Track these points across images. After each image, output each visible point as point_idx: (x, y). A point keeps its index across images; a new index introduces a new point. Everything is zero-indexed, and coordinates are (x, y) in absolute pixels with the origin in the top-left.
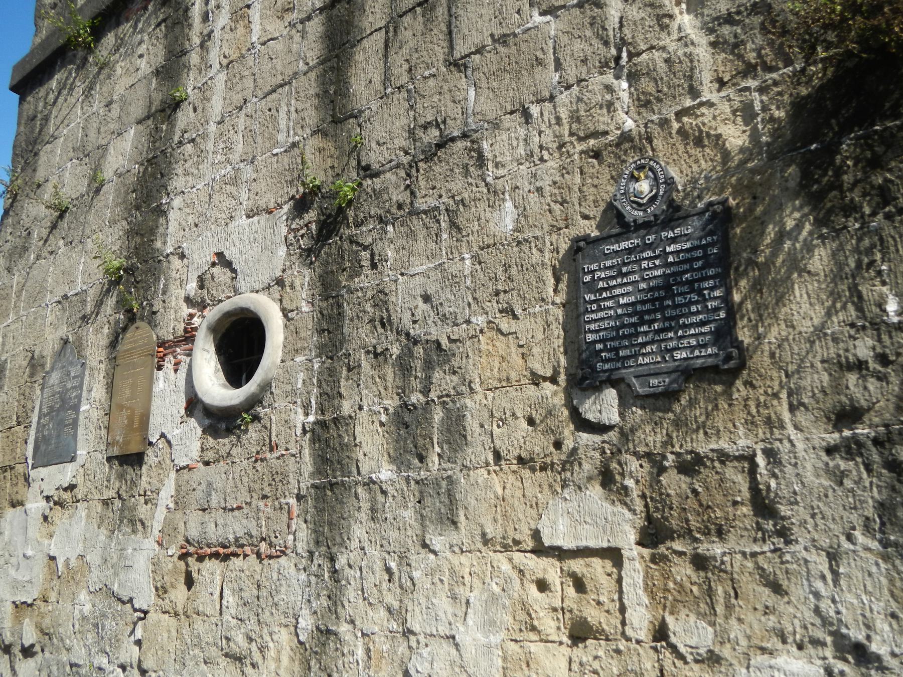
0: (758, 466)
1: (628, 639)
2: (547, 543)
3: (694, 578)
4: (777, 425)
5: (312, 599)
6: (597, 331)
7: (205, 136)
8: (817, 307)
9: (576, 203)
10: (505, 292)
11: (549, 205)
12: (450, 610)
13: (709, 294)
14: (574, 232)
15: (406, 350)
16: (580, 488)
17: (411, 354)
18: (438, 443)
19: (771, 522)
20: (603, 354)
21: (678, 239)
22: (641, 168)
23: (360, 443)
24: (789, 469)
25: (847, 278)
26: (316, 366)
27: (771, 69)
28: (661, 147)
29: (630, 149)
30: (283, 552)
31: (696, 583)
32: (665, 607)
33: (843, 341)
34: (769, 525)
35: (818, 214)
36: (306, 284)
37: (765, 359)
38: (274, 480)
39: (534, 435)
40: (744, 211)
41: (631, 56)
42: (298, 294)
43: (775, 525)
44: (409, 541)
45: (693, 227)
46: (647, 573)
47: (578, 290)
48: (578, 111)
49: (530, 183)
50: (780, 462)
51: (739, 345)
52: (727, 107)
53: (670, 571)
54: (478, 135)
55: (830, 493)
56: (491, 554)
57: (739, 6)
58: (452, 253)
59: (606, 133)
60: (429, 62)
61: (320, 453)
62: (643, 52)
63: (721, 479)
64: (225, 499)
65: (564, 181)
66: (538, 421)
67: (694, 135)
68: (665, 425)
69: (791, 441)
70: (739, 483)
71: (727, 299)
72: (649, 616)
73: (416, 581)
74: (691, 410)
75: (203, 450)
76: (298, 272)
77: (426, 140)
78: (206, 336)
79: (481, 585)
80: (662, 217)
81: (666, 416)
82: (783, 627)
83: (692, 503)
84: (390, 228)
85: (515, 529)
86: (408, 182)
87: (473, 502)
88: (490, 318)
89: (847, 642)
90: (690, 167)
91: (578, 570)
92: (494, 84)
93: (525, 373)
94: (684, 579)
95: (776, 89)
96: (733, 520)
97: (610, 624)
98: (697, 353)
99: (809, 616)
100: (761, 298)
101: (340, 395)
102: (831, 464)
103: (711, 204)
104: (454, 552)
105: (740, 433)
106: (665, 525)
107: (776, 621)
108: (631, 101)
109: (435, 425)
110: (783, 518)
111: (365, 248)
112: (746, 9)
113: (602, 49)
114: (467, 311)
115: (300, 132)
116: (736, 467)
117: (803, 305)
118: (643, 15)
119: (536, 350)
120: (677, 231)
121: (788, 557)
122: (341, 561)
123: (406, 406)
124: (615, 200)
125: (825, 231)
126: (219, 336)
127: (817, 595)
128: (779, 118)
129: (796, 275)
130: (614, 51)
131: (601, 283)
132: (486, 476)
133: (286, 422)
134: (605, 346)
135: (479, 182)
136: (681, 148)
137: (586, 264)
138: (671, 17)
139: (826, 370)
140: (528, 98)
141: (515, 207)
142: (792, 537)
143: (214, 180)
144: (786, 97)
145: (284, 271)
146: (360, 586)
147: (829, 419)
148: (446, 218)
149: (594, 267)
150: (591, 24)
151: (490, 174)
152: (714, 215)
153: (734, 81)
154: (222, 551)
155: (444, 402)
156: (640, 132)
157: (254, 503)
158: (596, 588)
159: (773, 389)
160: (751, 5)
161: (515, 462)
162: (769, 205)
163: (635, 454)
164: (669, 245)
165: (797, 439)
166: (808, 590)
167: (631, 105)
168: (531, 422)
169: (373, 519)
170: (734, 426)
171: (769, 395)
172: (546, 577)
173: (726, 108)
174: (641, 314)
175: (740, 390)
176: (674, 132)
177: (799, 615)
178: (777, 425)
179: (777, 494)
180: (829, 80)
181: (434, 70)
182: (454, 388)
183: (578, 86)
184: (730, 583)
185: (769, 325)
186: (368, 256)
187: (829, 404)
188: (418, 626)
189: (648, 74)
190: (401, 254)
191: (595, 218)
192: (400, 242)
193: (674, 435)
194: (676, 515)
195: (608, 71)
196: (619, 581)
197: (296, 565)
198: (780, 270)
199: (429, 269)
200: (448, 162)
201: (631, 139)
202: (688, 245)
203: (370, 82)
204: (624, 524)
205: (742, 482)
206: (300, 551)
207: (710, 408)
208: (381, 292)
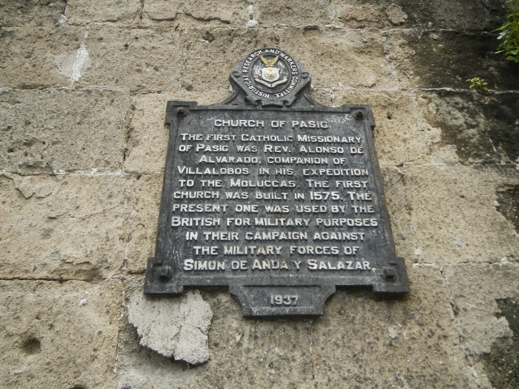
98: (340, 265)
131: (204, 156)
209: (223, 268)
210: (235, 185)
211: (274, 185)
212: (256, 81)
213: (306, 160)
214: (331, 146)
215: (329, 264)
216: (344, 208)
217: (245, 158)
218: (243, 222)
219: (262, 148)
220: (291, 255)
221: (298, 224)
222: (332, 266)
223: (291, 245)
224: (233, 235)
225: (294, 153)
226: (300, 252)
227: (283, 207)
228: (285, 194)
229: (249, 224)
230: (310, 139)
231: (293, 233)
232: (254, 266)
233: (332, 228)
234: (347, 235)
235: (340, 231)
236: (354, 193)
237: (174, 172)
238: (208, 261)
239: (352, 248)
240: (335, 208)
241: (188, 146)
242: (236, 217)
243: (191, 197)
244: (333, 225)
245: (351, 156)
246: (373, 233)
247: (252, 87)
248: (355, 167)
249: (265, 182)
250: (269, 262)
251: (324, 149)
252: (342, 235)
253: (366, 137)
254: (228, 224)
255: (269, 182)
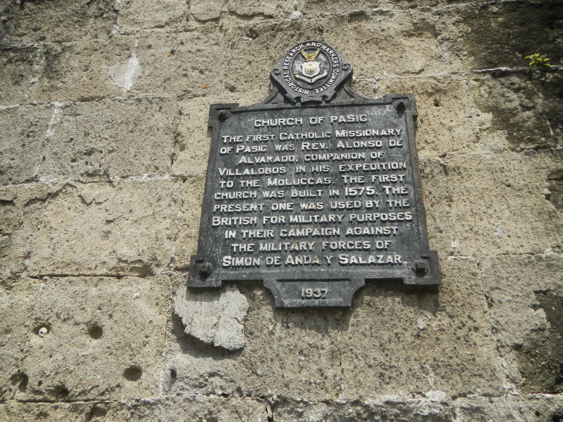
6: (230, 214)
98: (371, 259)
131: (243, 157)
209: (258, 264)
210: (272, 184)
211: (309, 183)
212: (296, 78)
213: (342, 155)
214: (369, 140)
215: (360, 259)
216: (378, 202)
217: (283, 157)
218: (278, 220)
219: (300, 146)
220: (323, 250)
221: (332, 220)
222: (363, 260)
223: (323, 240)
224: (268, 233)
225: (332, 149)
226: (332, 247)
227: (318, 204)
228: (320, 191)
229: (284, 221)
230: (348, 134)
231: (326, 230)
232: (287, 262)
233: (365, 223)
234: (380, 230)
235: (373, 226)
236: (390, 187)
237: (215, 173)
238: (245, 257)
239: (384, 242)
240: (369, 203)
241: (228, 148)
242: (272, 215)
243: (230, 197)
244: (366, 220)
245: (389, 150)
246: (407, 227)
247: (292, 84)
248: (393, 161)
249: (301, 180)
250: (301, 257)
251: (362, 143)
252: (375, 230)
253: (407, 129)
254: (264, 223)
255: (305, 179)
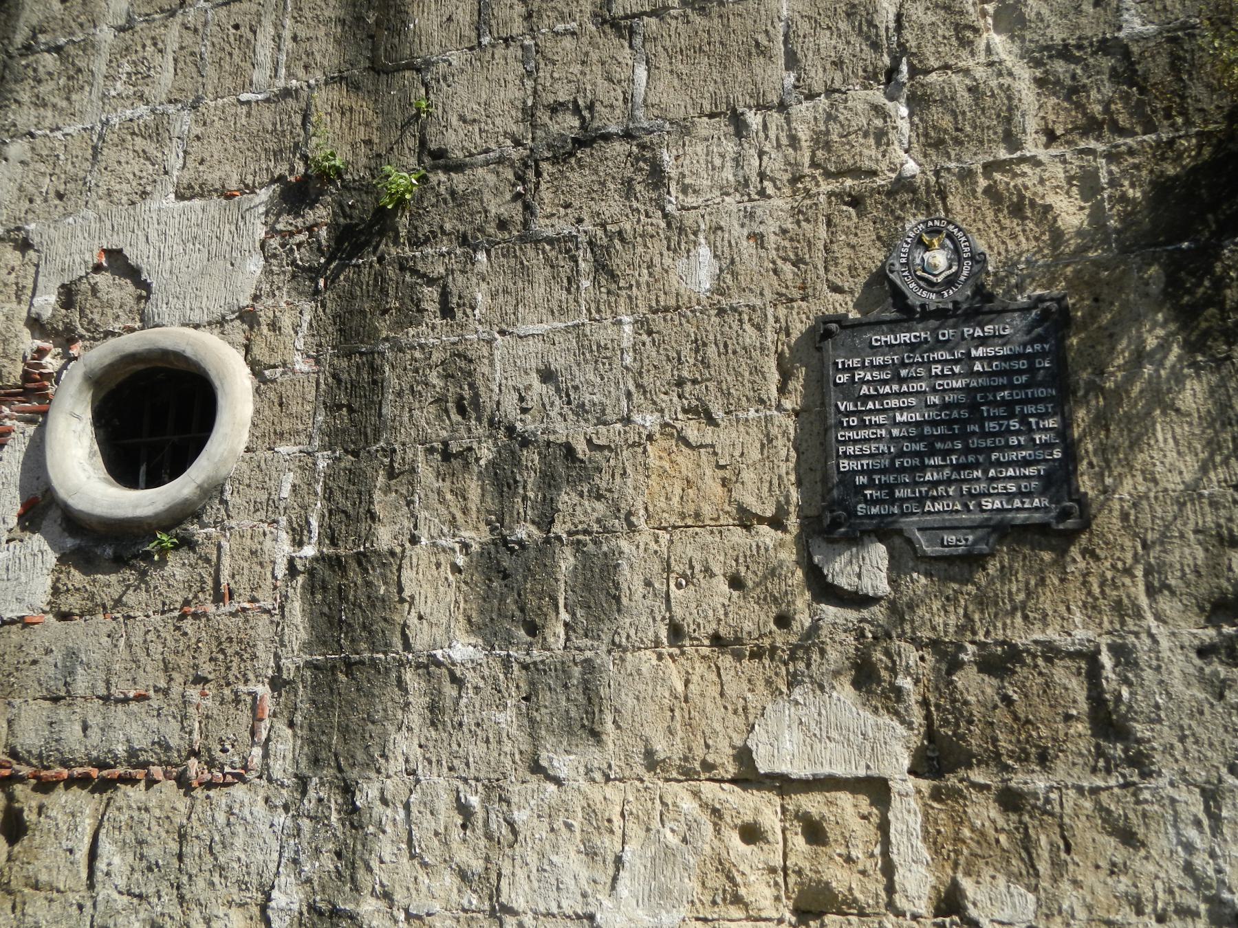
0: (1103, 667)
1: (899, 913)
2: (763, 768)
3: (1001, 822)
4: (1130, 612)
5: (303, 857)
6: (856, 457)
7: (88, 46)
8: (1188, 458)
9: (821, 266)
10: (694, 382)
11: (774, 262)
12: (584, 874)
13: (1037, 423)
14: (816, 308)
15: (505, 454)
16: (822, 688)
17: (516, 461)
18: (566, 606)
19: (1119, 746)
20: (868, 492)
21: (990, 342)
22: (935, 232)
23: (412, 597)
24: (1148, 674)
25: (1230, 424)
26: (322, 464)
27: (1122, 132)
28: (959, 208)
29: (911, 202)
30: (241, 778)
31: (1003, 829)
32: (956, 866)
33: (1225, 507)
34: (1118, 750)
35: (1190, 334)
36: (305, 325)
37: (1114, 521)
38: (222, 651)
39: (742, 604)
40: (1083, 316)
41: (913, 71)
42: (287, 340)
43: (1126, 751)
44: (508, 762)
45: (1012, 327)
46: (926, 815)
47: (824, 395)
48: (828, 133)
49: (743, 226)
50: (1136, 664)
51: (1082, 501)
52: (1061, 170)
53: (965, 812)
54: (655, 137)
55: (1206, 708)
56: (660, 783)
57: (1080, 38)
58: (599, 311)
59: (874, 173)
60: (566, 10)
61: (326, 610)
62: (934, 70)
63: (1047, 684)
64: (108, 682)
65: (800, 232)
66: (750, 584)
67: (1010, 199)
68: (962, 602)
69: (1151, 636)
70: (1074, 690)
71: (1063, 433)
72: (932, 880)
73: (519, 826)
74: (1003, 584)
75: (56, 591)
76: (288, 303)
77: (554, 128)
78: (80, 391)
79: (643, 834)
80: (965, 306)
81: (964, 589)
82: (1140, 891)
83: (1001, 715)
84: (481, 256)
85: (707, 746)
86: (520, 188)
87: (631, 702)
88: (667, 419)
89: (1227, 911)
90: (1004, 243)
91: (813, 811)
92: (681, 68)
93: (727, 508)
94: (987, 824)
95: (1131, 160)
96: (1064, 741)
97: (868, 890)
98: (1017, 503)
99: (1177, 876)
100: (1107, 437)
101: (373, 517)
102: (1207, 670)
103: (1040, 299)
104: (593, 780)
105: (1077, 620)
106: (960, 746)
107: (1130, 883)
108: (914, 135)
109: (561, 577)
110: (1139, 741)
111: (431, 282)
112: (1091, 45)
113: (868, 53)
114: (624, 403)
115: (301, 73)
116: (1068, 668)
117: (1168, 454)
118: (934, 19)
119: (748, 476)
120: (989, 329)
121: (1146, 795)
122: (367, 794)
123: (505, 542)
124: (892, 272)
125: (1200, 358)
126: (102, 394)
127: (1189, 847)
128: (1134, 198)
129: (1158, 412)
130: (886, 60)
131: (865, 387)
132: (654, 662)
133: (253, 553)
134: (871, 480)
135: (651, 210)
136: (990, 216)
137: (839, 357)
138: (976, 30)
139: (1200, 544)
140: (742, 101)
141: (716, 256)
142: (1153, 768)
143: (105, 123)
144: (1144, 173)
145: (256, 298)
146: (405, 837)
147: (1202, 609)
148: (589, 255)
149: (854, 362)
150: (848, 15)
151: (673, 199)
152: (1046, 313)
153: (1069, 137)
154: (95, 773)
155: (579, 542)
156: (927, 182)
157: (176, 689)
158: (844, 837)
159: (1124, 563)
160: (1098, 41)
161: (707, 642)
162: (1119, 313)
163: (915, 641)
164: (976, 348)
165: (1161, 633)
166: (1175, 841)
167: (914, 139)
168: (736, 582)
169: (433, 724)
170: (1068, 609)
171: (1118, 570)
172: (760, 819)
173: (1058, 171)
174: (931, 440)
175: (1077, 562)
176: (979, 190)
177: (1162, 875)
178: (1130, 612)
179: (1130, 707)
180: (1205, 162)
181: (574, 24)
182: (598, 521)
183: (827, 97)
184: (1057, 830)
185: (1120, 474)
186: (436, 296)
187: (1203, 590)
188: (521, 900)
189: (941, 101)
190: (501, 299)
191: (852, 292)
192: (498, 282)
193: (977, 617)
194: (977, 731)
195: (875, 86)
196: (884, 827)
197: (267, 800)
198: (1136, 404)
199: (555, 331)
200: (596, 172)
201: (914, 190)
202: (1006, 351)
203: (450, 19)
204: (894, 742)
205: (1077, 688)
206: (277, 774)
207: (1033, 582)
208: (459, 355)
